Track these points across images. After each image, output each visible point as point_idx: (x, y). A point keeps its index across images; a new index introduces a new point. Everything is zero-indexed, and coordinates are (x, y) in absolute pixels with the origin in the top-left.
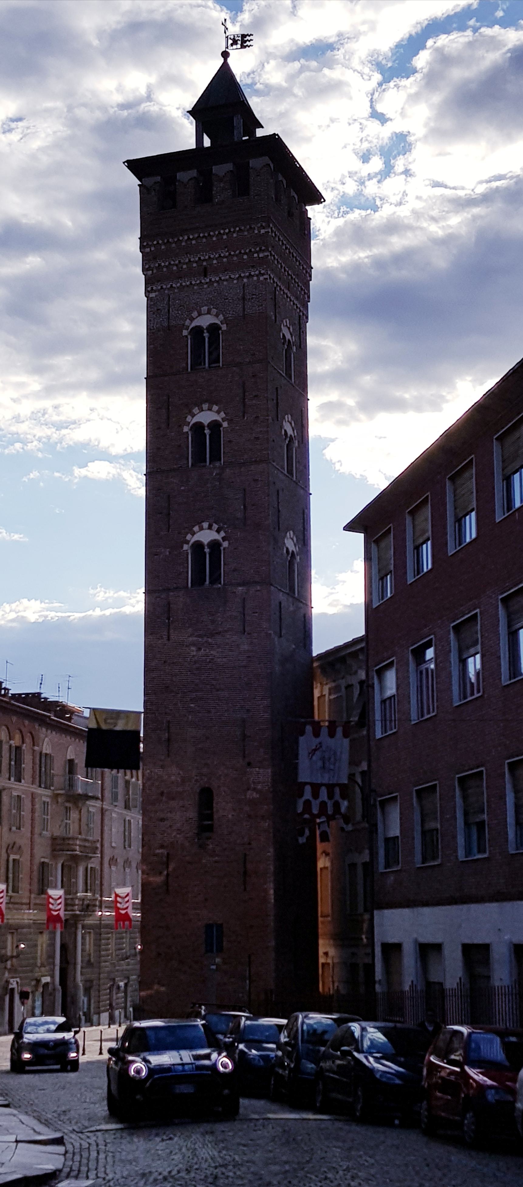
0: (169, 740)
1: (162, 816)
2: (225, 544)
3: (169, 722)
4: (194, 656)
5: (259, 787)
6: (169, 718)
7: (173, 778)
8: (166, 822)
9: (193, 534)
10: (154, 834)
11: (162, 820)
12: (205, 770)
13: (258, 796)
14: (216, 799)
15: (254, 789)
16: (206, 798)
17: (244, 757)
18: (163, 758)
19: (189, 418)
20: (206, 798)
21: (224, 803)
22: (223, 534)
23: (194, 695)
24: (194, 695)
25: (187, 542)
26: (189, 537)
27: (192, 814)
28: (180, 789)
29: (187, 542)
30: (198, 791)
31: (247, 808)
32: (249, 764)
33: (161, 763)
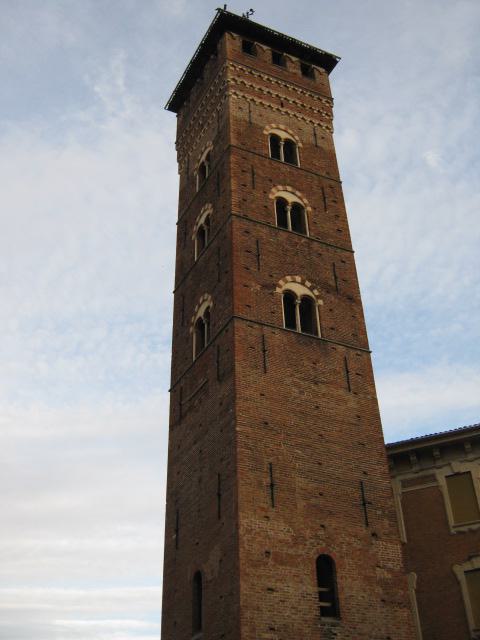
0: (272, 485)
1: (270, 585)
2: (321, 302)
3: (270, 464)
4: (295, 398)
5: (390, 565)
6: (271, 460)
7: (281, 536)
8: (275, 594)
9: (286, 282)
10: (258, 609)
11: (271, 590)
12: (321, 533)
13: (390, 576)
14: (340, 573)
15: (384, 567)
16: (325, 569)
17: (367, 525)
18: (265, 506)
19: (273, 190)
20: (325, 569)
21: (350, 580)
22: (316, 292)
23: (300, 440)
24: (300, 440)
25: (280, 287)
26: (281, 282)
27: (311, 588)
28: (291, 551)
29: (280, 287)
30: (315, 557)
31: (379, 590)
32: (374, 535)
33: (264, 514)
